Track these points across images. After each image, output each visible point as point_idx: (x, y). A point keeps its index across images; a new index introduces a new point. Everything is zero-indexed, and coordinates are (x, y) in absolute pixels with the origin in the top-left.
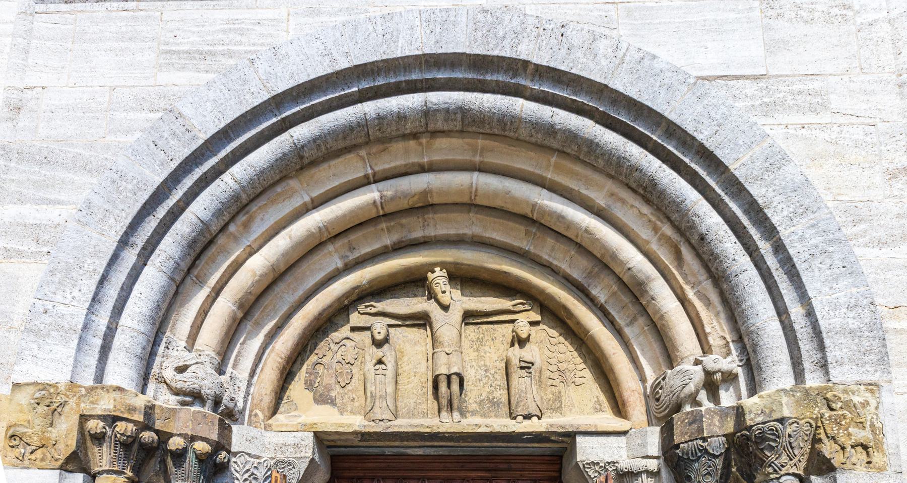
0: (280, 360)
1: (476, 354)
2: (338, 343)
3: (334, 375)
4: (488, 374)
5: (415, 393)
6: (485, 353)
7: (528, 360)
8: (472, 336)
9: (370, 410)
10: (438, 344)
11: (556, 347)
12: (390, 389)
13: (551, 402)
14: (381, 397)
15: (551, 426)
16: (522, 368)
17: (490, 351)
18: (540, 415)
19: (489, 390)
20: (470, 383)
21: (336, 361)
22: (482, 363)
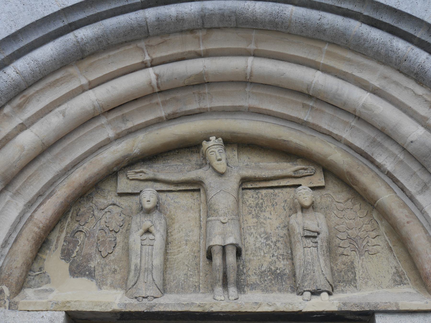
0: (36, 229)
1: (255, 220)
2: (103, 210)
3: (95, 244)
4: (269, 242)
5: (186, 263)
6: (265, 219)
7: (314, 229)
8: (250, 202)
9: (133, 286)
10: (213, 212)
11: (344, 213)
12: (157, 261)
13: (343, 273)
14: (146, 270)
15: (345, 304)
16: (307, 237)
17: (270, 217)
18: (330, 290)
19: (270, 260)
20: (249, 252)
21: (99, 228)
22: (262, 230)
